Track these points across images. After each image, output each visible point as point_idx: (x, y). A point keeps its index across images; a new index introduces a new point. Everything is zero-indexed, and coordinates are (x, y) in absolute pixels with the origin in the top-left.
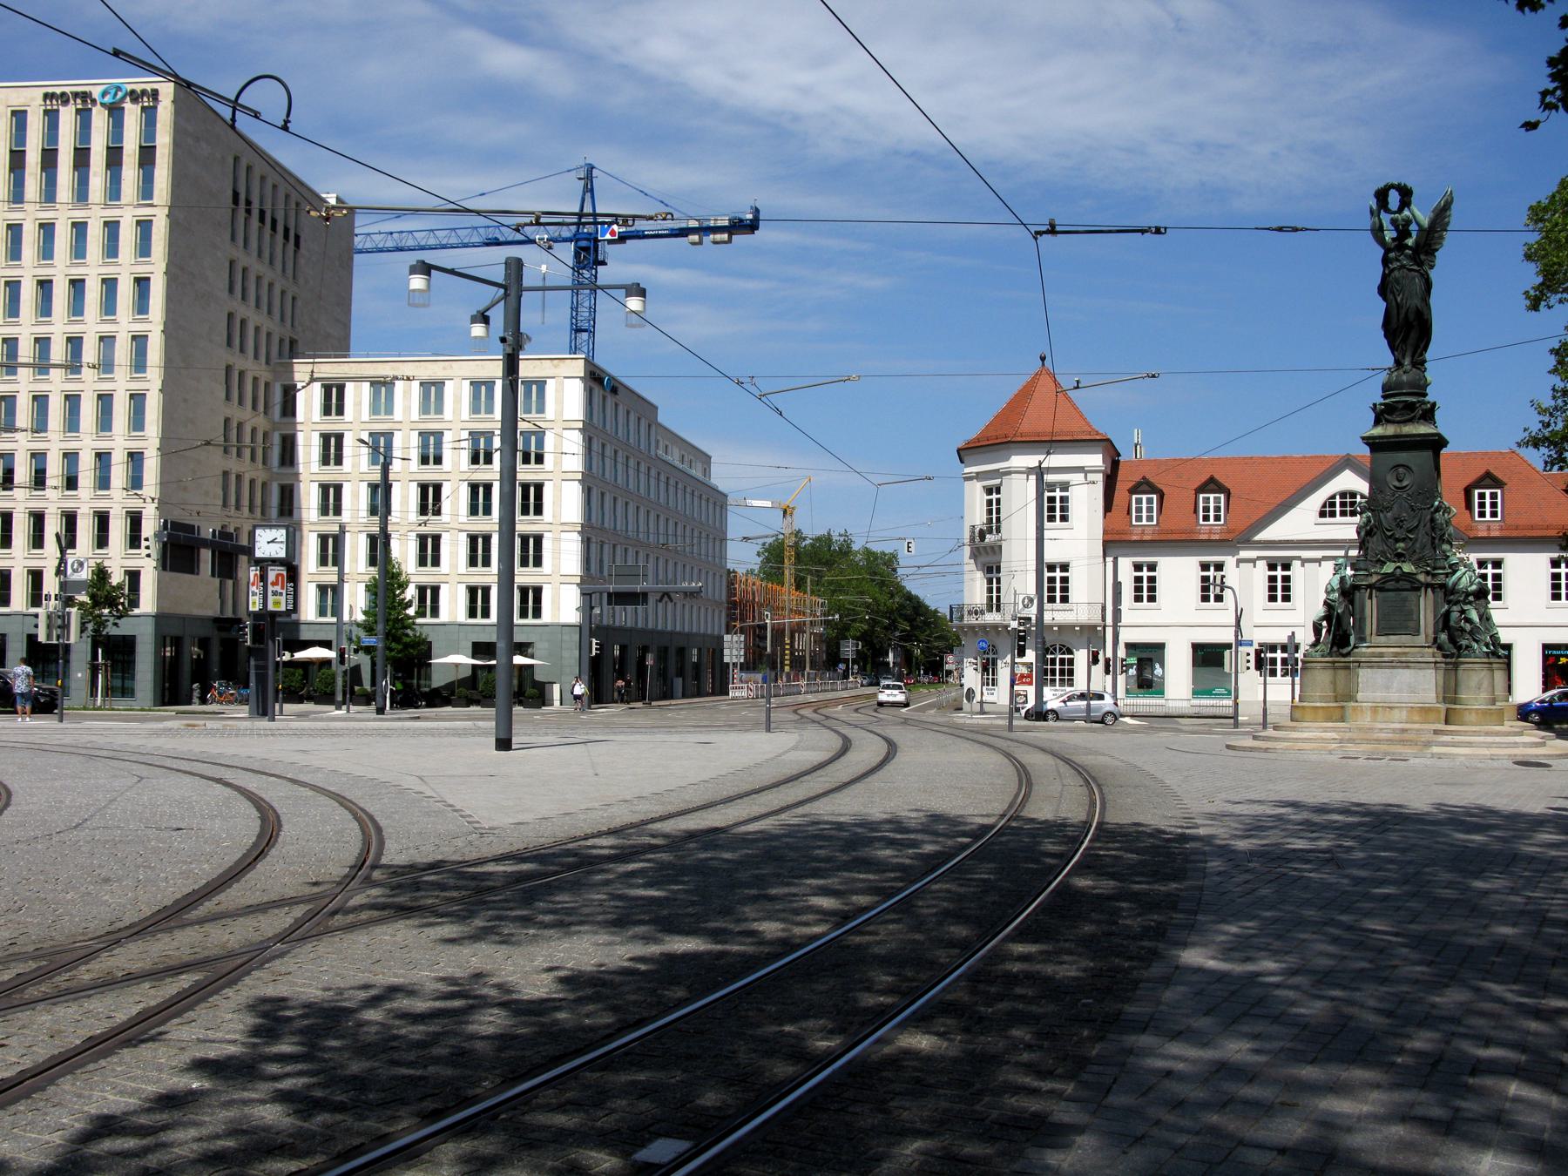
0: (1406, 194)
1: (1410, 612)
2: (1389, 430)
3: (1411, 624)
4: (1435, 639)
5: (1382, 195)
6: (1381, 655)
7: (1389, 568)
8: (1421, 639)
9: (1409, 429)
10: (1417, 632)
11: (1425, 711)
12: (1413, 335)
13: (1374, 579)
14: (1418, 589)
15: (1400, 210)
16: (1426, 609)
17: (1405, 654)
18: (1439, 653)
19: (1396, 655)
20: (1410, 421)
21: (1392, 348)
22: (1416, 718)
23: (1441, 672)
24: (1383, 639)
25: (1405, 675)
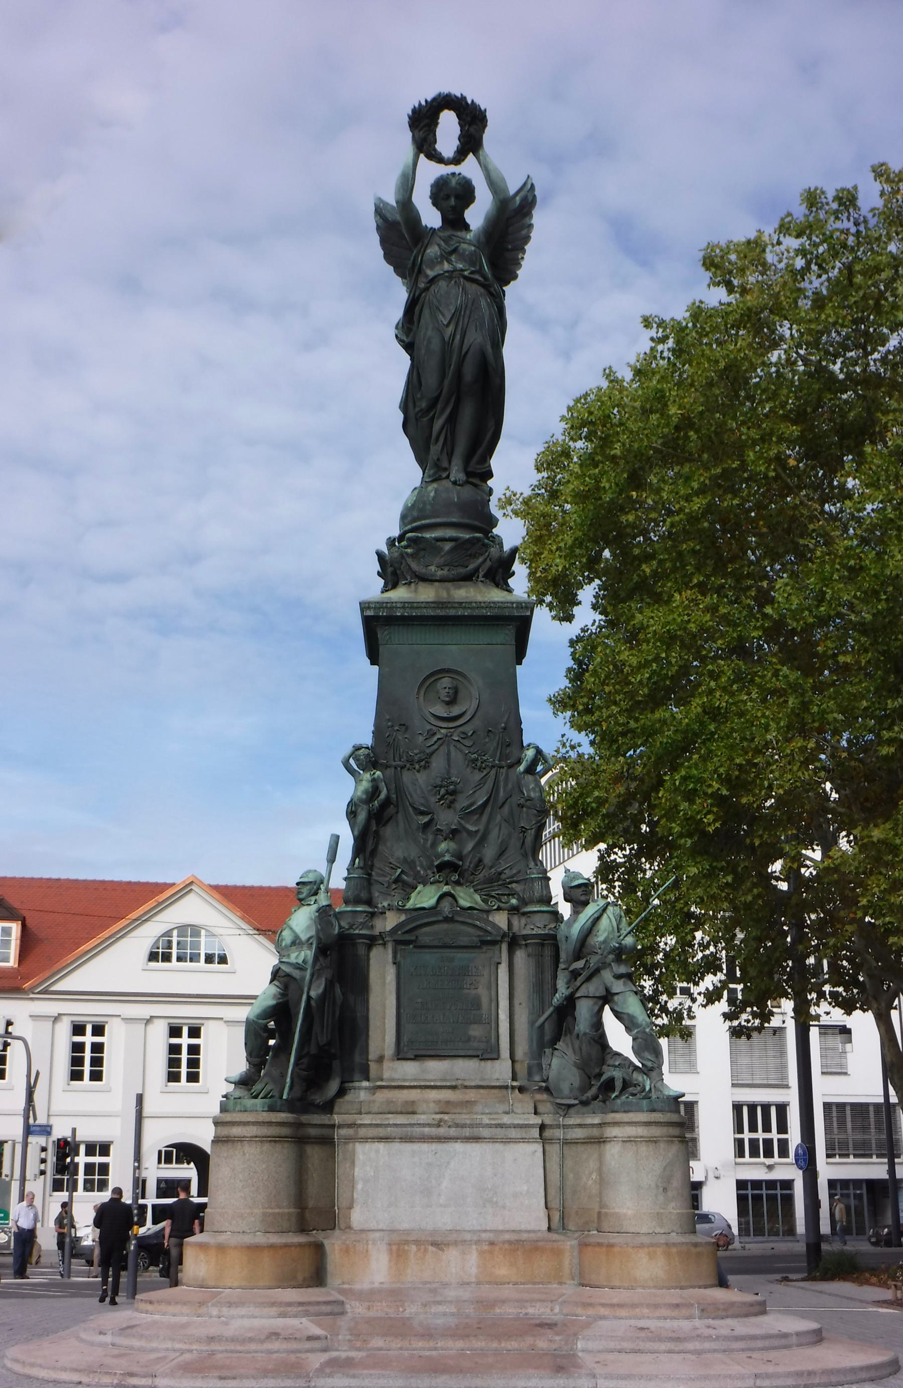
0: (473, 120)
1: (476, 1004)
2: (426, 594)
3: (476, 1031)
4: (536, 1067)
5: (423, 121)
6: (410, 1109)
7: (425, 897)
8: (501, 1070)
9: (463, 593)
10: (490, 1053)
11: (520, 1247)
12: (467, 414)
13: (390, 921)
14: (494, 943)
15: (459, 158)
16: (507, 996)
17: (468, 1104)
18: (546, 1107)
19: (446, 1108)
20: (468, 578)
21: (421, 458)
22: (503, 1271)
23: (554, 1150)
24: (409, 1070)
25: (467, 1161)
